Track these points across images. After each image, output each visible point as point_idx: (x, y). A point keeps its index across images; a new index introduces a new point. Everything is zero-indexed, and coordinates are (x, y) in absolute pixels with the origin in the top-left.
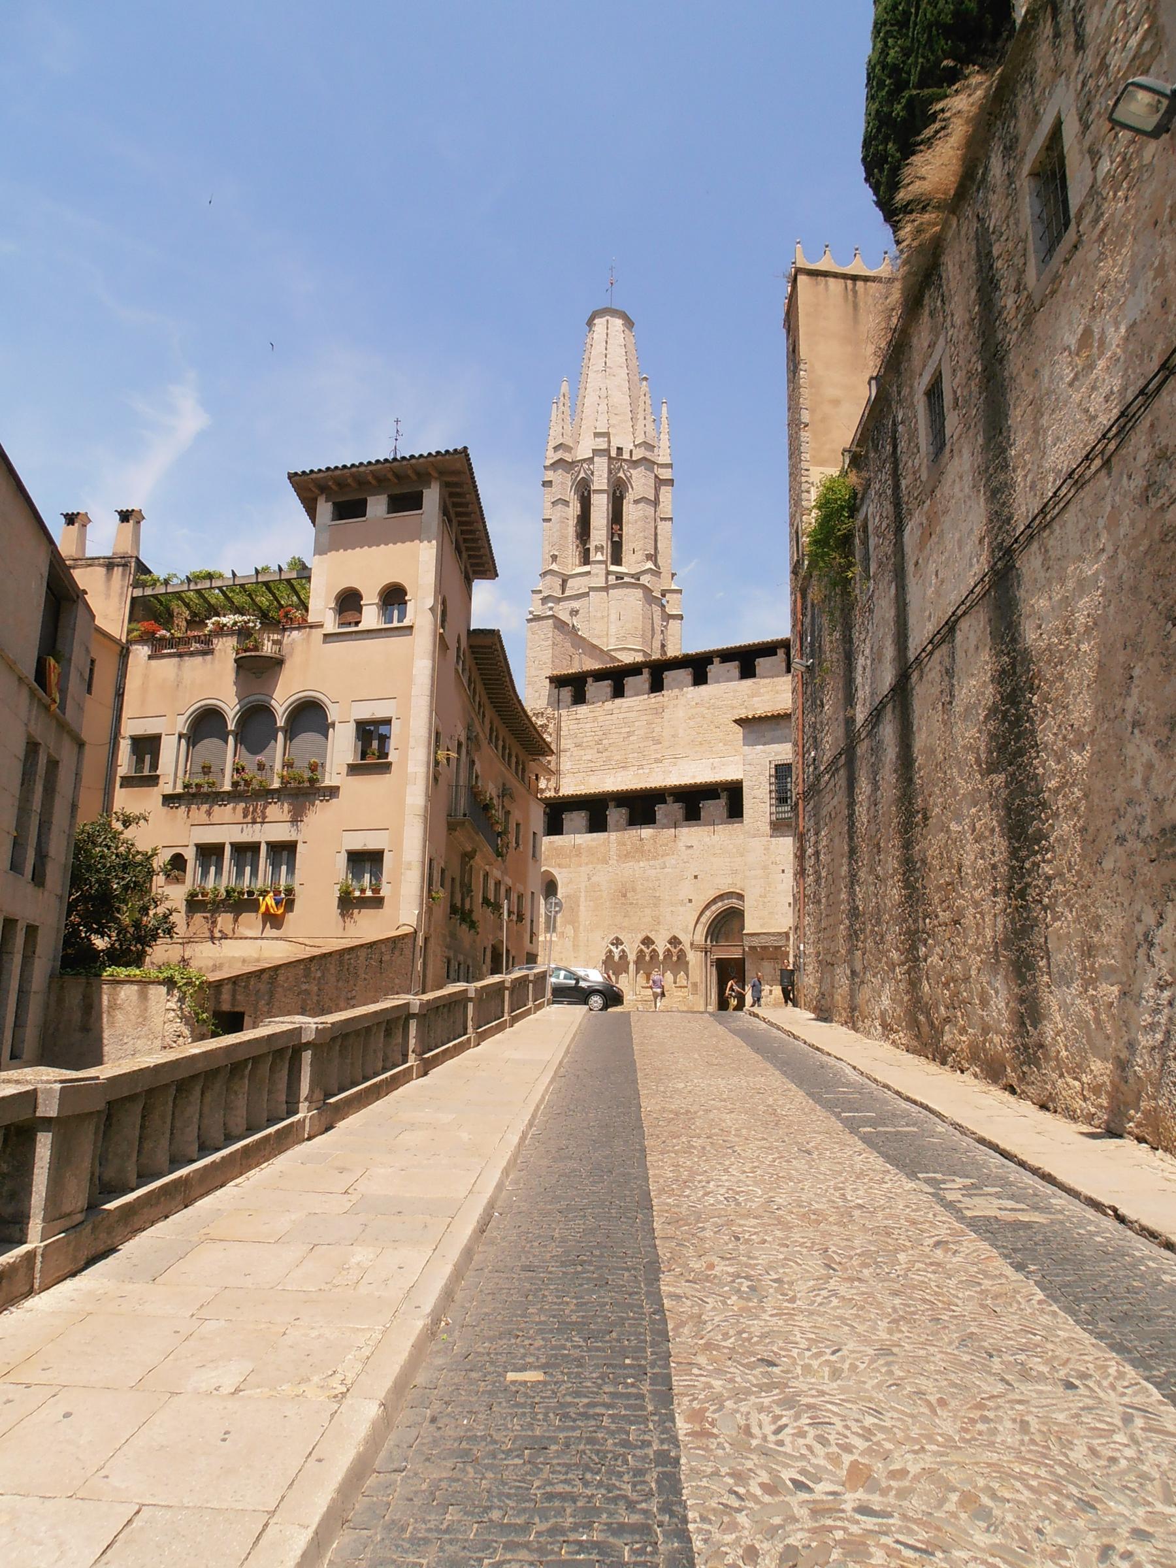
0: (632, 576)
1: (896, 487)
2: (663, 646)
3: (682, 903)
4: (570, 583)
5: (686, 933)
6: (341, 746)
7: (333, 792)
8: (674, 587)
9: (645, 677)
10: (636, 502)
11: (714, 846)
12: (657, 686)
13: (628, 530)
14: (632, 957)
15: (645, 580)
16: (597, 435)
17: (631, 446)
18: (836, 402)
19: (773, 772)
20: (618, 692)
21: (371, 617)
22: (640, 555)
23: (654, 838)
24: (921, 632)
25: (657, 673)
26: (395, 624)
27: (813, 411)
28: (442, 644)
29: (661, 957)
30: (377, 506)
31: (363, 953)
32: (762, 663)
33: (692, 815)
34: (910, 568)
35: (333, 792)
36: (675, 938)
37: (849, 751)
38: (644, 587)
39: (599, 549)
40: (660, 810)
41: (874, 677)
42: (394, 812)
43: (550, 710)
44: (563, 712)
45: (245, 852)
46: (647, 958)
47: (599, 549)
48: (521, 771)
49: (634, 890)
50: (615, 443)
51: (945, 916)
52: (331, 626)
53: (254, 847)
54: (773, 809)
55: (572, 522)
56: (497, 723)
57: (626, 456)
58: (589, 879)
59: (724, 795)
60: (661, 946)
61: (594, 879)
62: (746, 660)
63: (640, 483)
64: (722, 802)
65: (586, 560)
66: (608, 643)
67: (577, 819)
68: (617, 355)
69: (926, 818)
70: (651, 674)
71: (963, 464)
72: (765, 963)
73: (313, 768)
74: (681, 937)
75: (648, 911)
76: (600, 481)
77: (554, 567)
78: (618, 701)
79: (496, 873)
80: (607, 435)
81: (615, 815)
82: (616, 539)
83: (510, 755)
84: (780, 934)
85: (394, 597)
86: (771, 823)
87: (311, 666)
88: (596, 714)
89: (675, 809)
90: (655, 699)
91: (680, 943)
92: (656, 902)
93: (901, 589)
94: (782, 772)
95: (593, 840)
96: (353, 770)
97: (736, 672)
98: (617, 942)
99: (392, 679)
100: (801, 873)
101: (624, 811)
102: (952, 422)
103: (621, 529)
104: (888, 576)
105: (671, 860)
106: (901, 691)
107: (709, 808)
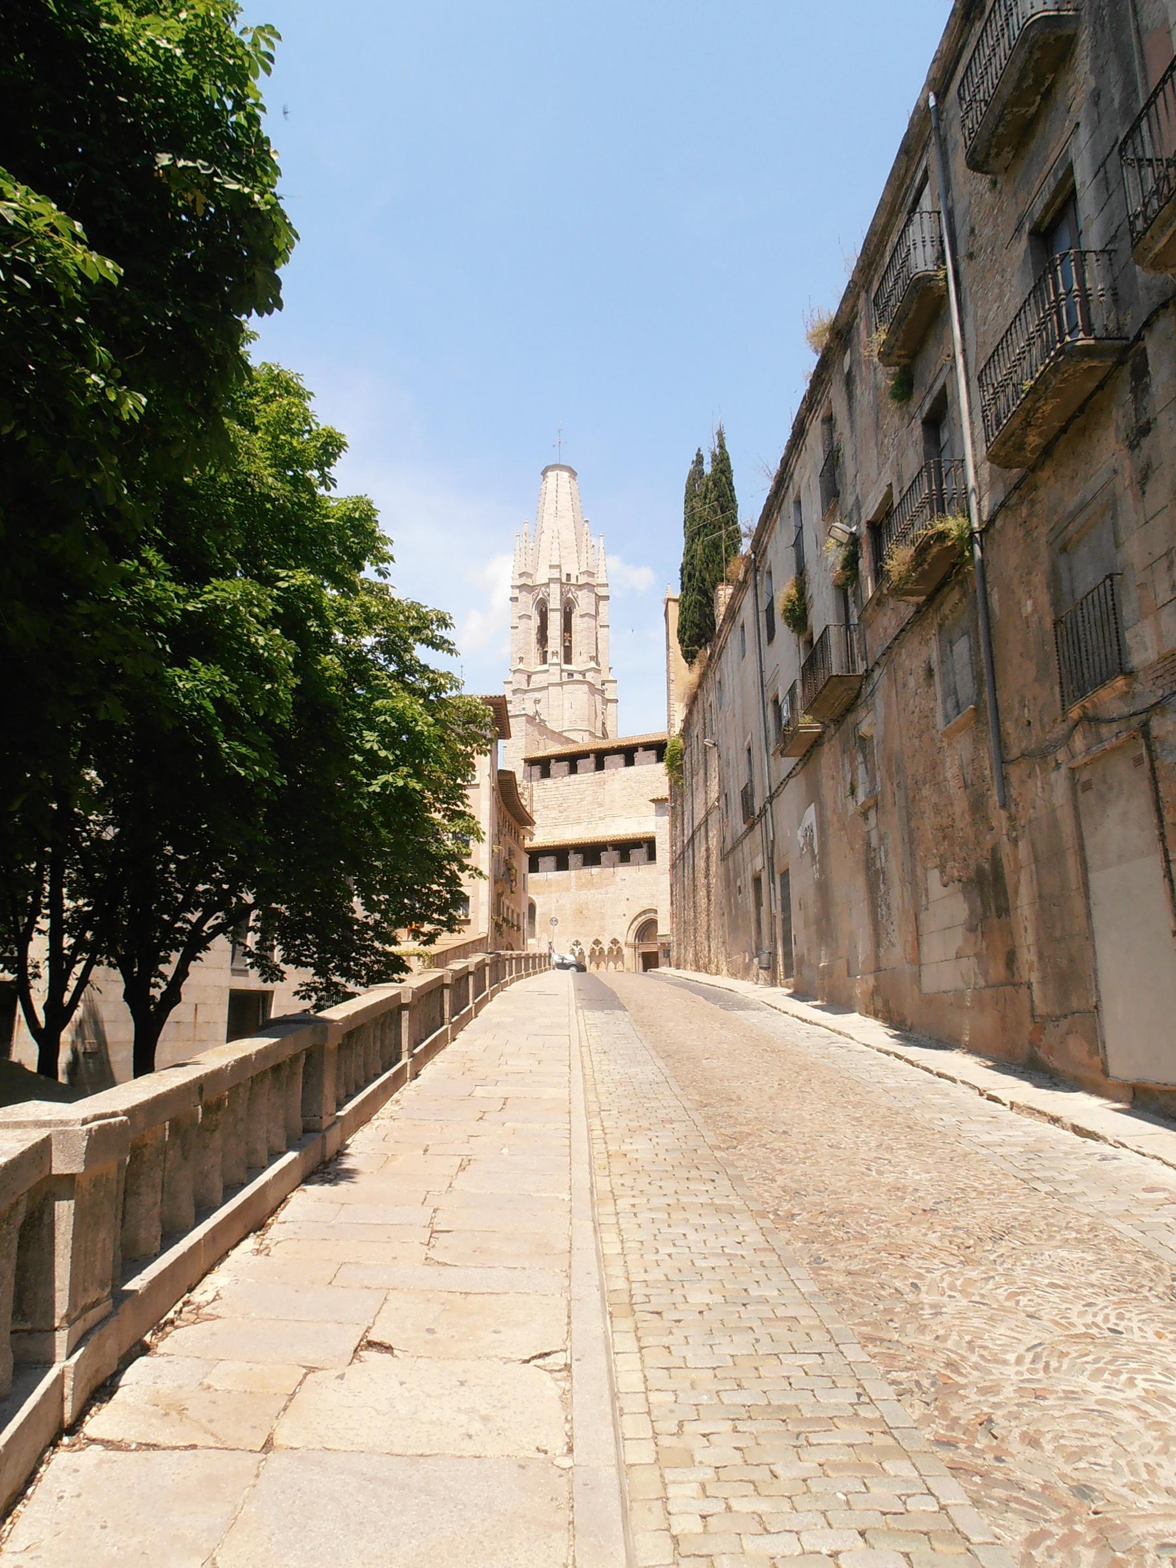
0: (580, 673)
2: (604, 724)
3: (619, 916)
4: (533, 678)
5: (622, 935)
8: (611, 678)
10: (582, 616)
12: (600, 766)
13: (576, 637)
14: (587, 953)
15: (590, 677)
16: (551, 567)
20: (573, 770)
22: (585, 657)
24: (696, 823)
25: (600, 758)
27: (676, 674)
33: (625, 859)
39: (555, 654)
40: (604, 855)
41: (688, 832)
47: (555, 654)
48: (517, 837)
50: (565, 571)
56: (507, 812)
57: (573, 581)
59: (645, 845)
60: (606, 945)
61: (561, 902)
63: (584, 603)
64: (644, 850)
65: (544, 661)
67: (550, 861)
71: (702, 772)
76: (555, 603)
77: (521, 666)
78: (573, 776)
79: (507, 902)
80: (559, 567)
81: (574, 859)
89: (614, 855)
97: (654, 758)
98: (577, 943)
100: (672, 904)
101: (580, 856)
107: (635, 854)
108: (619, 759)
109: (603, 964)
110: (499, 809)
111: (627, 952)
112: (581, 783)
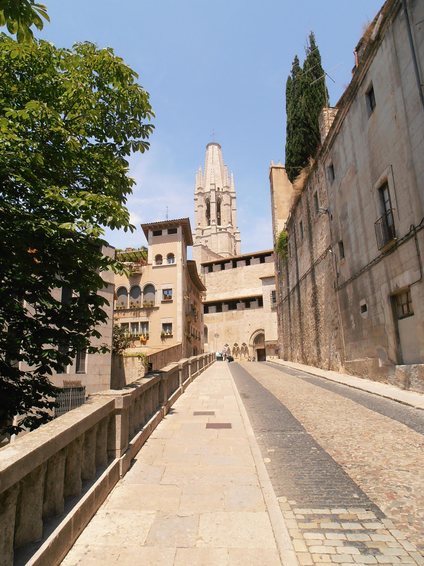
0: (224, 229)
1: (295, 240)
2: (235, 250)
6: (159, 297)
7: (158, 308)
9: (231, 264)
10: (224, 205)
12: (235, 266)
13: (222, 214)
14: (231, 350)
15: (228, 230)
16: (211, 184)
17: (222, 187)
18: (283, 202)
19: (271, 293)
20: (223, 268)
21: (165, 262)
22: (227, 222)
23: (237, 313)
24: (301, 275)
25: (235, 262)
26: (171, 264)
27: (277, 205)
29: (240, 349)
30: (165, 232)
31: (172, 349)
32: (267, 258)
33: (248, 306)
34: (299, 260)
35: (158, 308)
36: (244, 343)
37: (289, 296)
38: (228, 233)
40: (238, 305)
41: (293, 282)
42: (174, 313)
43: (202, 274)
44: (206, 275)
45: (135, 325)
46: (236, 350)
48: (198, 296)
49: (231, 329)
50: (217, 187)
51: (307, 335)
52: (154, 265)
53: (137, 324)
54: (272, 304)
55: (204, 212)
56: (192, 284)
57: (221, 190)
62: (262, 257)
63: (225, 199)
65: (209, 225)
66: (217, 251)
67: (213, 308)
68: (216, 158)
69: (303, 314)
70: (233, 262)
71: (306, 243)
72: (271, 349)
73: (152, 302)
76: (213, 199)
77: (199, 227)
78: (223, 271)
79: (193, 326)
80: (214, 184)
81: (224, 307)
82: (219, 217)
84: (275, 341)
86: (271, 308)
87: (149, 275)
89: (243, 304)
90: (234, 270)
93: (297, 263)
94: (273, 293)
96: (163, 302)
97: (259, 261)
98: (227, 345)
100: (279, 325)
102: (304, 233)
103: (220, 214)
104: (294, 259)
105: (242, 320)
106: (298, 285)
107: (252, 304)
108: (243, 262)
109: (239, 355)
110: (188, 281)
111: (250, 349)
112: (227, 273)
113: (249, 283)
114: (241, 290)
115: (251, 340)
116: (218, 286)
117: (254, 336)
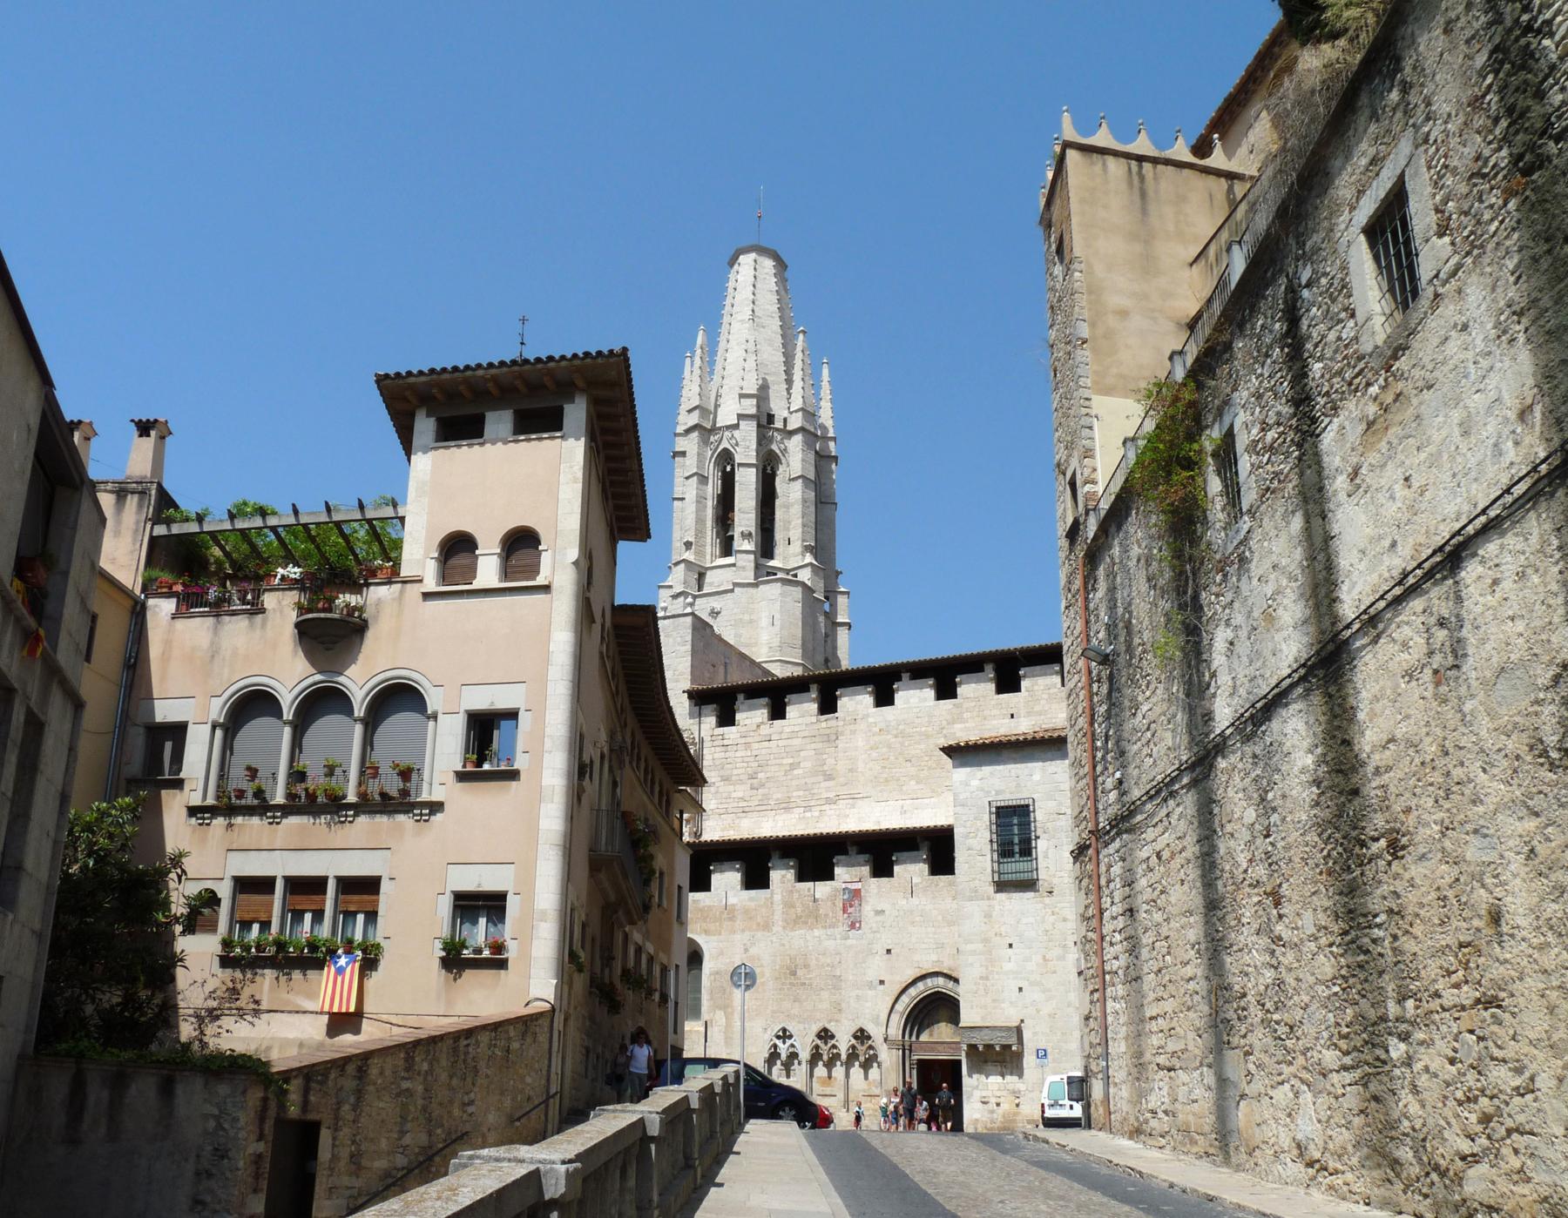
0: (787, 572)
3: (870, 985)
4: (710, 577)
5: (876, 1021)
6: (446, 745)
7: (436, 807)
11: (912, 912)
14: (805, 1055)
22: (797, 546)
28: (586, 612)
31: (484, 1038)
35: (436, 807)
36: (862, 1030)
42: (521, 839)
47: (746, 536)
48: (666, 804)
49: (806, 966)
58: (746, 950)
60: (844, 1042)
65: (727, 548)
66: (760, 655)
73: (405, 774)
74: (871, 1029)
75: (825, 995)
83: (653, 782)
85: (521, 544)
87: (406, 632)
88: (749, 740)
91: (869, 1037)
92: (836, 982)
95: (751, 899)
96: (462, 777)
98: (784, 1035)
99: (520, 656)
111: (888, 1057)
113: (887, 780)
114: (853, 806)
115: (895, 1018)
116: (752, 779)
117: (906, 1002)
